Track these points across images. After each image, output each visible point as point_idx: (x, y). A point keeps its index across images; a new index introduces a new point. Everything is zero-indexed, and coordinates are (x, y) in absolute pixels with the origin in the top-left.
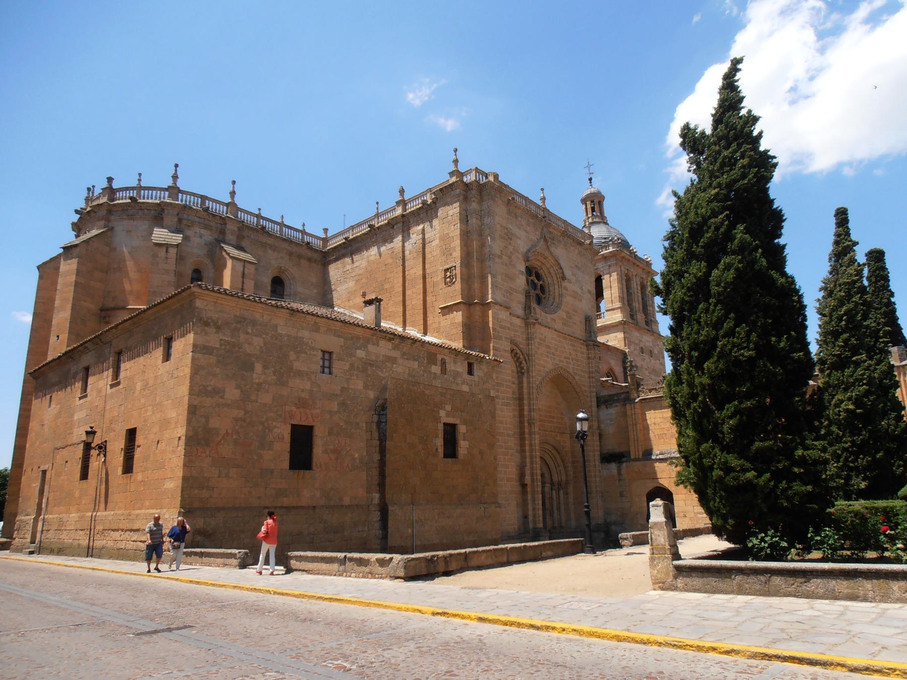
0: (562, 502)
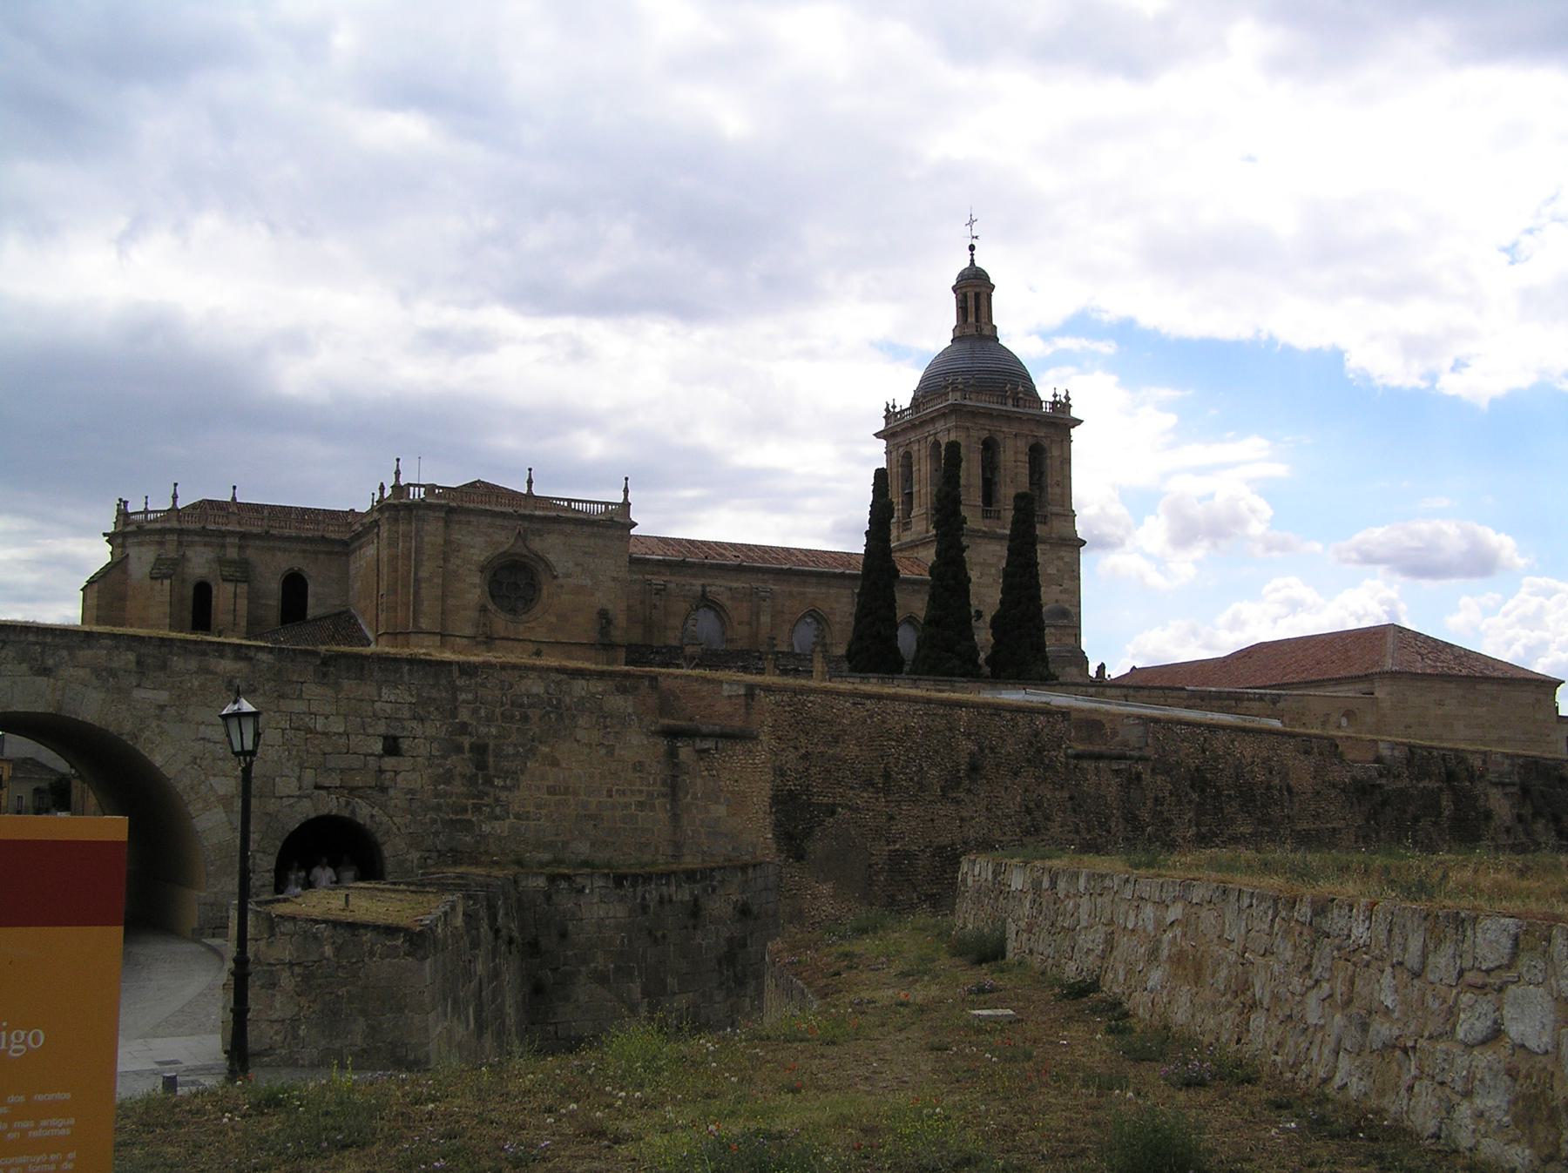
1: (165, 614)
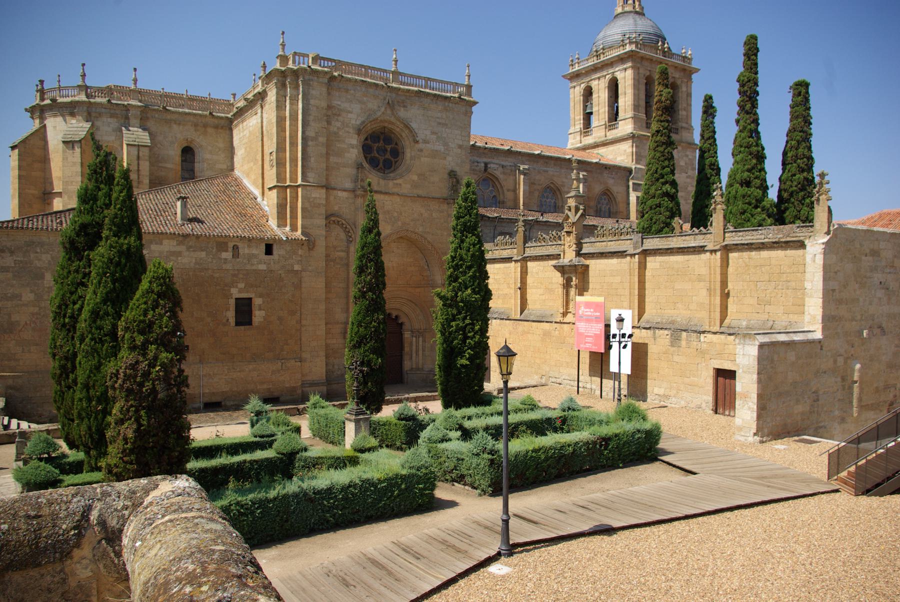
0: (421, 348)
1: (77, 172)
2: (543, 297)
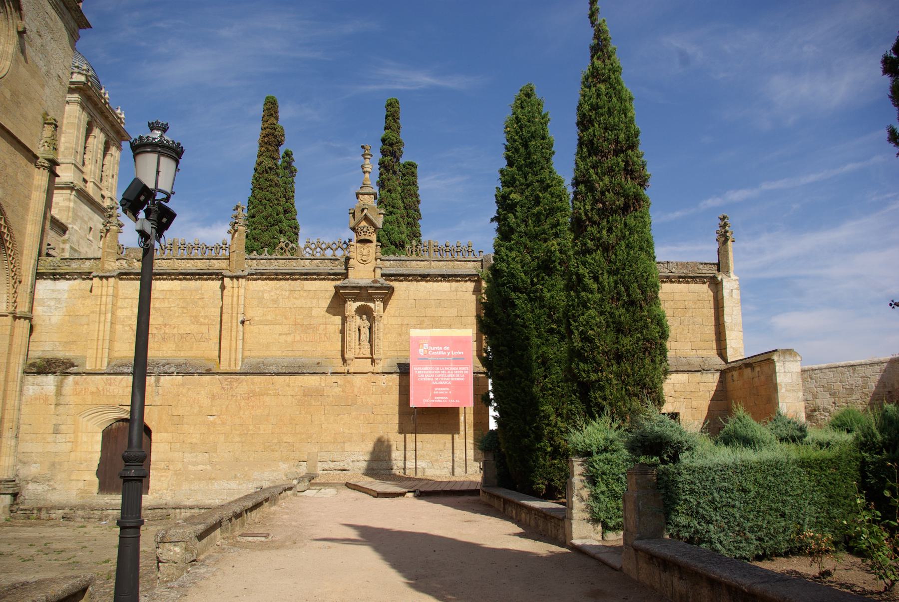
2: (289, 338)
